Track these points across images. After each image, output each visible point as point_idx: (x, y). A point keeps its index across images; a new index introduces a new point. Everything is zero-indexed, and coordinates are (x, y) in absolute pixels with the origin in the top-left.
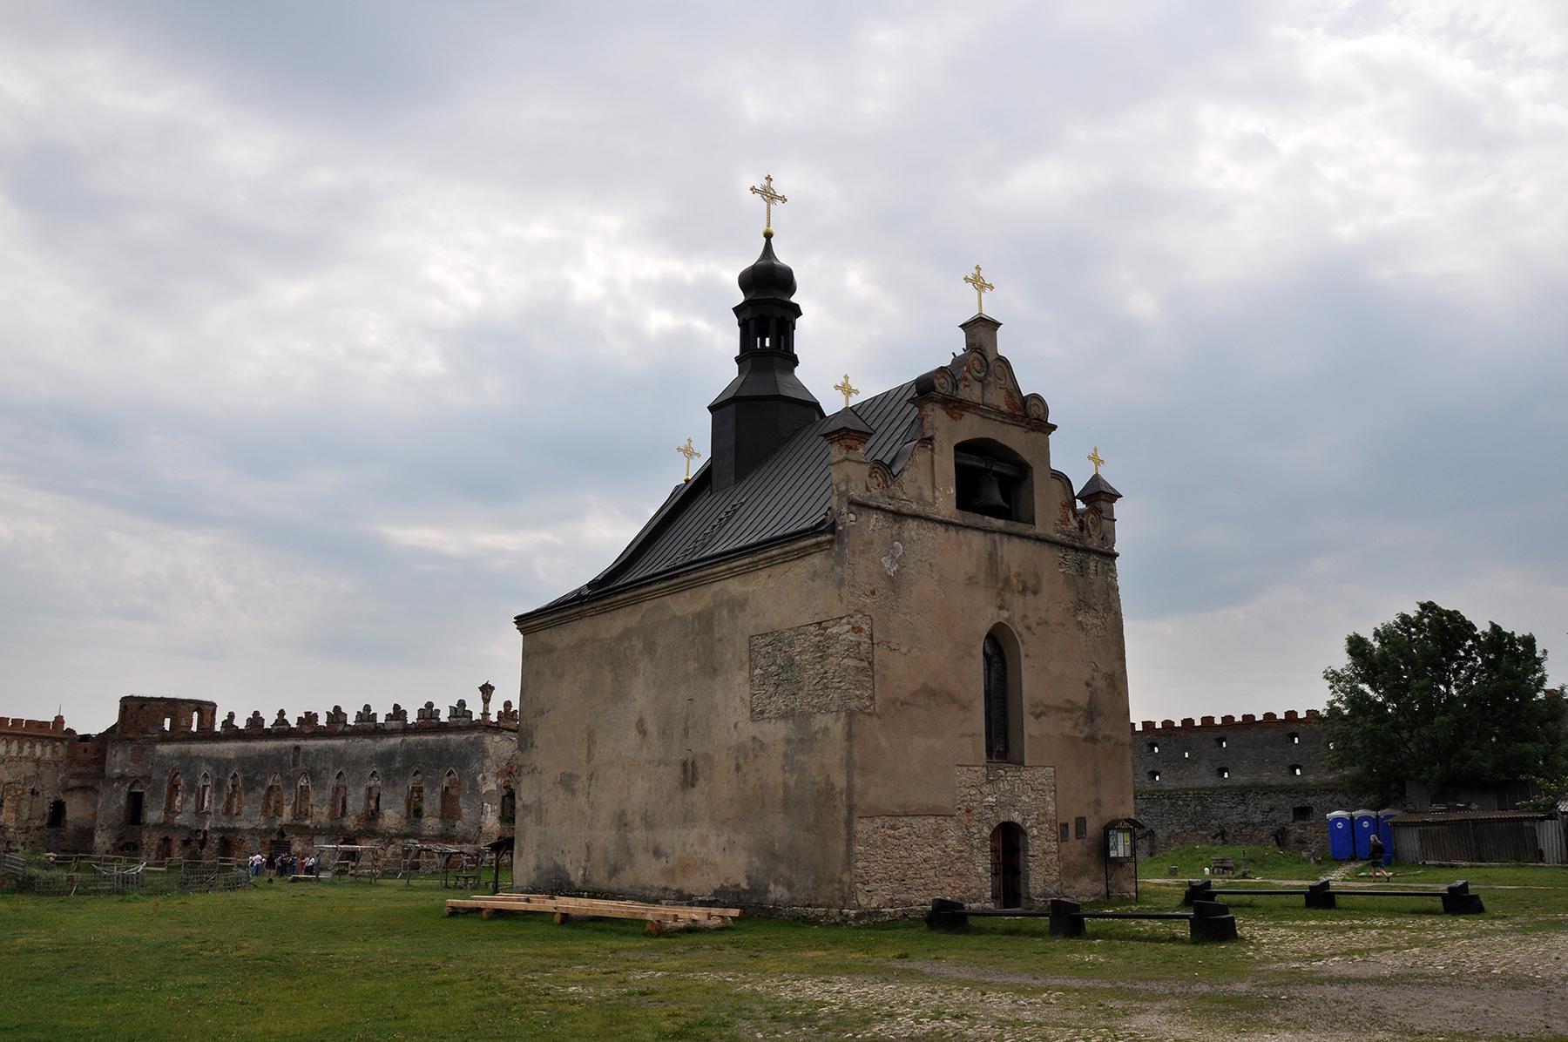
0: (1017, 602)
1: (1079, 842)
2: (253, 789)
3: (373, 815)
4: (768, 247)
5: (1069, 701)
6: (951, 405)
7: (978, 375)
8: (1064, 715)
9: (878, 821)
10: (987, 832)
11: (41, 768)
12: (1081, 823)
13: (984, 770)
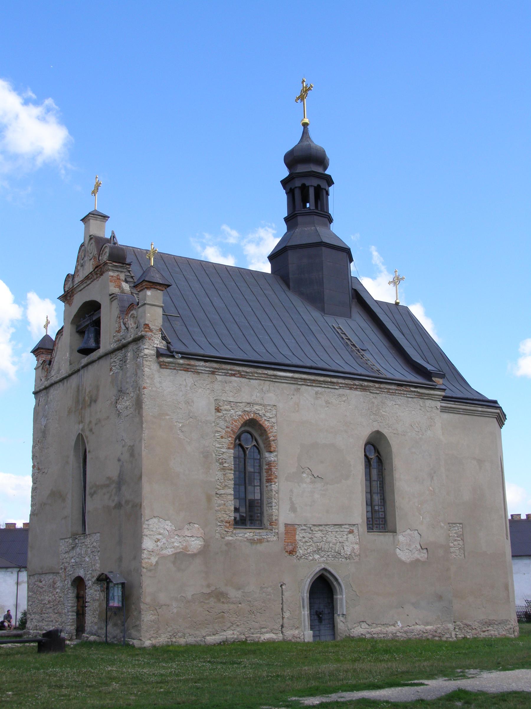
4: (305, 133)
5: (109, 478)
6: (68, 298)
9: (36, 577)
13: (71, 541)
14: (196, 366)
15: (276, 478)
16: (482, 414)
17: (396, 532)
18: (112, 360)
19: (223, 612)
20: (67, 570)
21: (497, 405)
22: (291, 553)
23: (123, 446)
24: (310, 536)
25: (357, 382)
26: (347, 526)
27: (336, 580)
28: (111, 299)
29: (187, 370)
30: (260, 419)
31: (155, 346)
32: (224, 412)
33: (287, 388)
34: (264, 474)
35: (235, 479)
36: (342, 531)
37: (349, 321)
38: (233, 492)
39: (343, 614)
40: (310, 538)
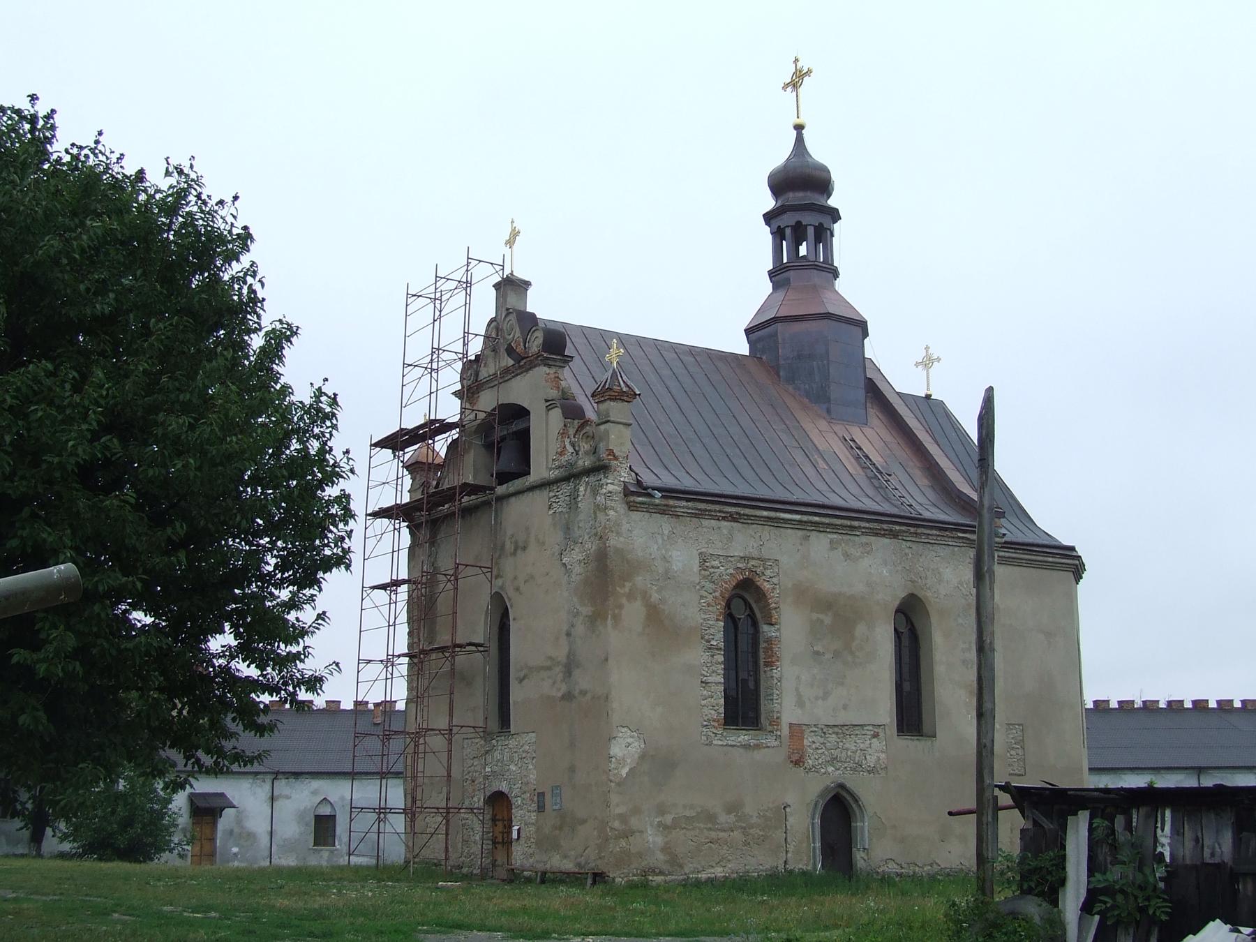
4: (800, 141)
5: (550, 658)
14: (676, 507)
15: (778, 661)
16: (1053, 567)
17: (935, 737)
18: (552, 494)
19: (711, 842)
20: (476, 783)
21: (1074, 554)
22: (797, 763)
24: (822, 740)
25: (885, 526)
26: (871, 728)
27: (856, 801)
28: (547, 407)
29: (663, 513)
30: (758, 579)
31: (622, 479)
32: (710, 570)
33: (792, 536)
34: (762, 655)
35: (724, 663)
36: (864, 735)
37: (867, 430)
38: (722, 680)
39: (865, 849)
40: (821, 744)
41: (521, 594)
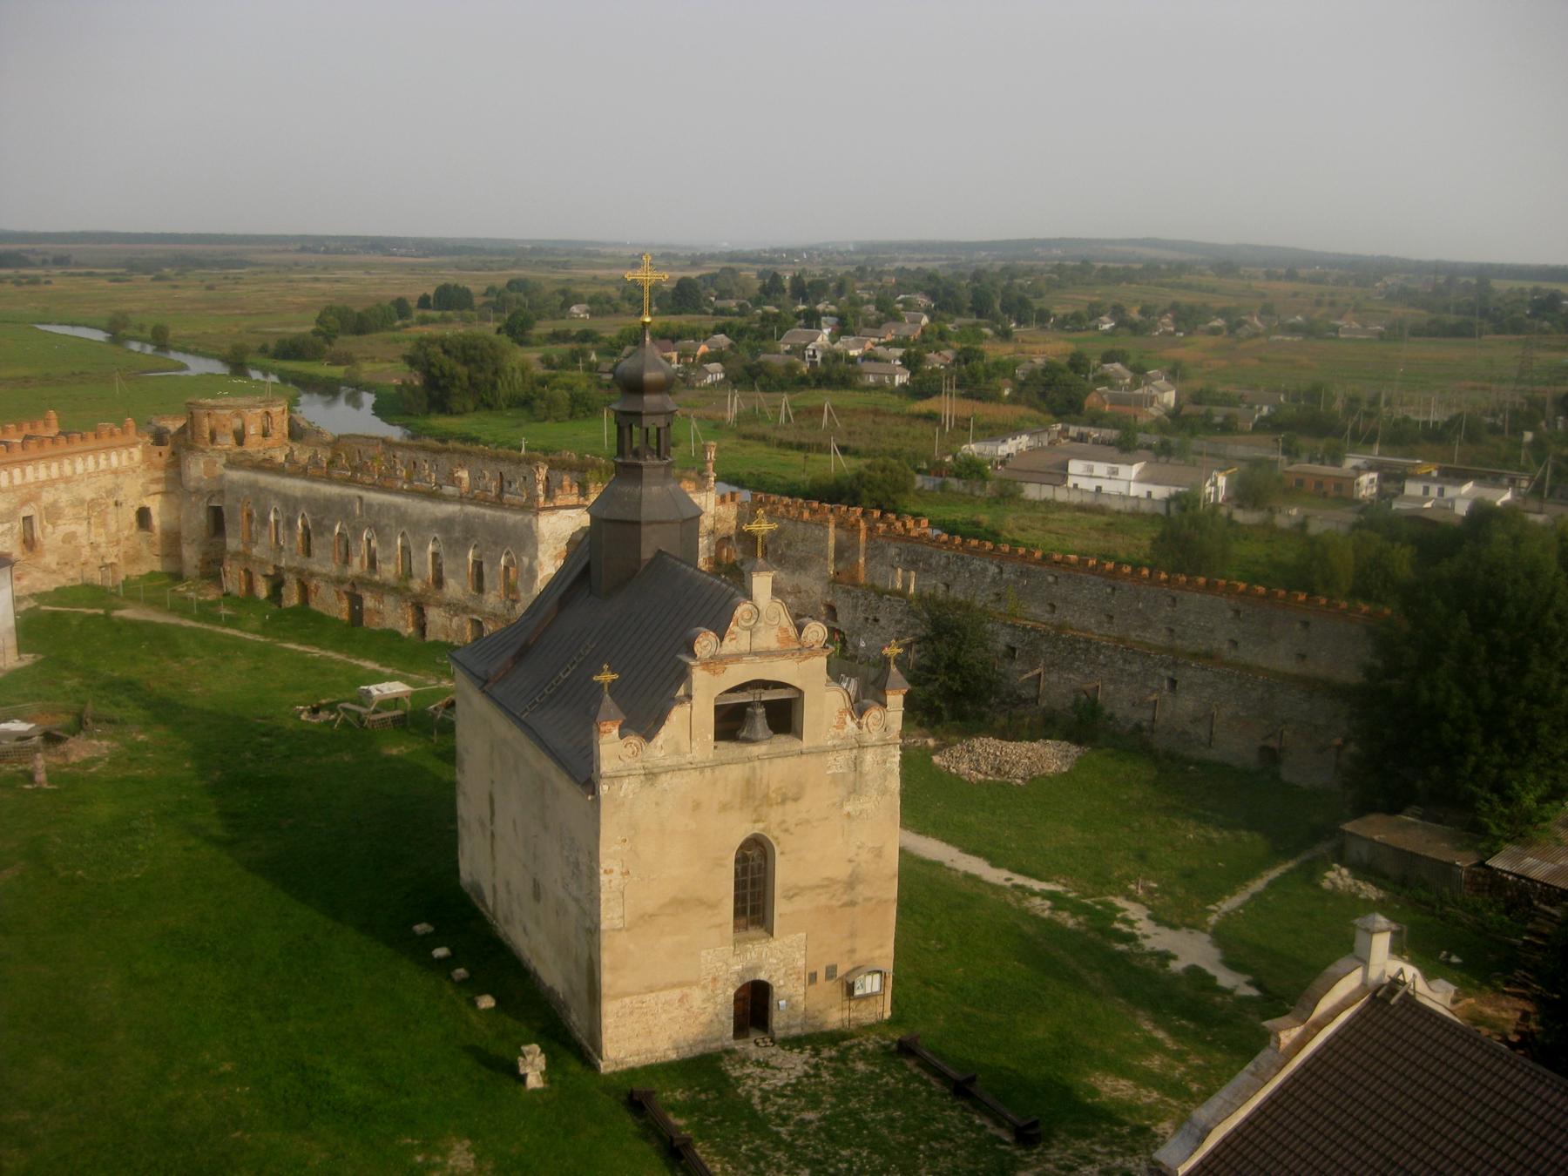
0: (775, 815)
1: (829, 983)
2: (322, 534)
3: (439, 581)
5: (828, 879)
7: (747, 625)
8: (818, 891)
9: (627, 1000)
10: (731, 992)
11: (119, 481)
12: (831, 972)
13: (732, 948)
23: (859, 848)
41: (792, 834)
